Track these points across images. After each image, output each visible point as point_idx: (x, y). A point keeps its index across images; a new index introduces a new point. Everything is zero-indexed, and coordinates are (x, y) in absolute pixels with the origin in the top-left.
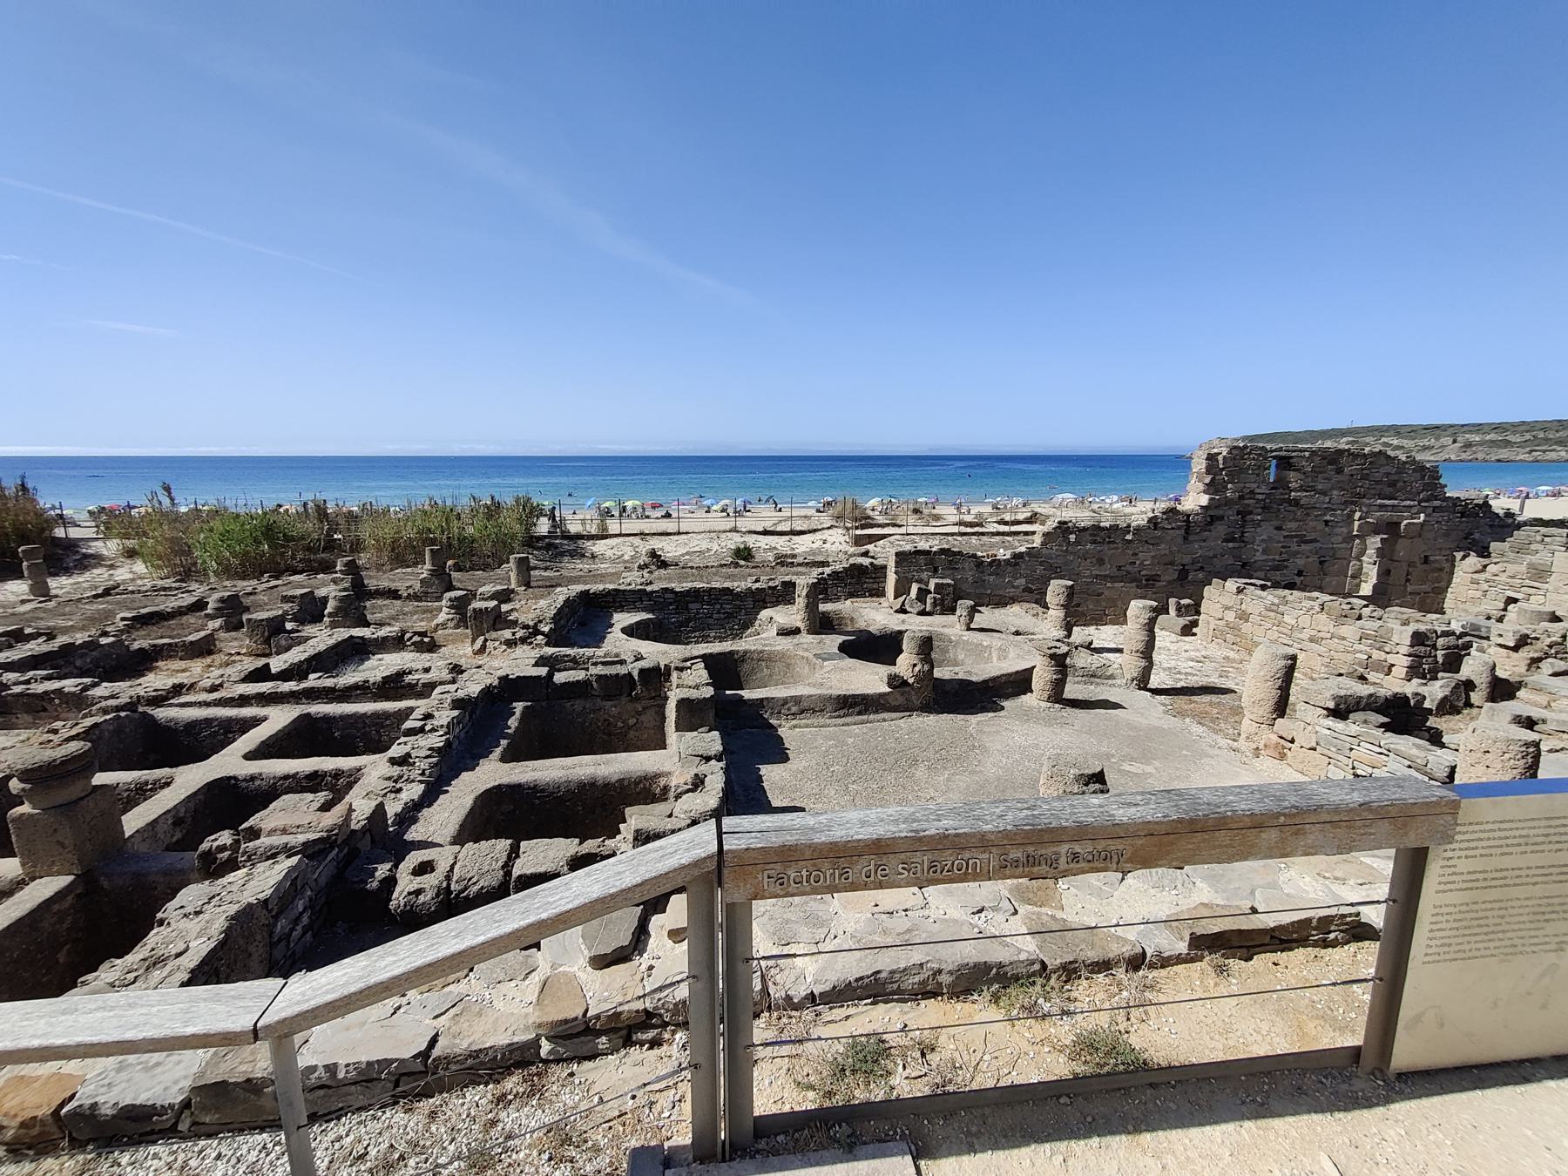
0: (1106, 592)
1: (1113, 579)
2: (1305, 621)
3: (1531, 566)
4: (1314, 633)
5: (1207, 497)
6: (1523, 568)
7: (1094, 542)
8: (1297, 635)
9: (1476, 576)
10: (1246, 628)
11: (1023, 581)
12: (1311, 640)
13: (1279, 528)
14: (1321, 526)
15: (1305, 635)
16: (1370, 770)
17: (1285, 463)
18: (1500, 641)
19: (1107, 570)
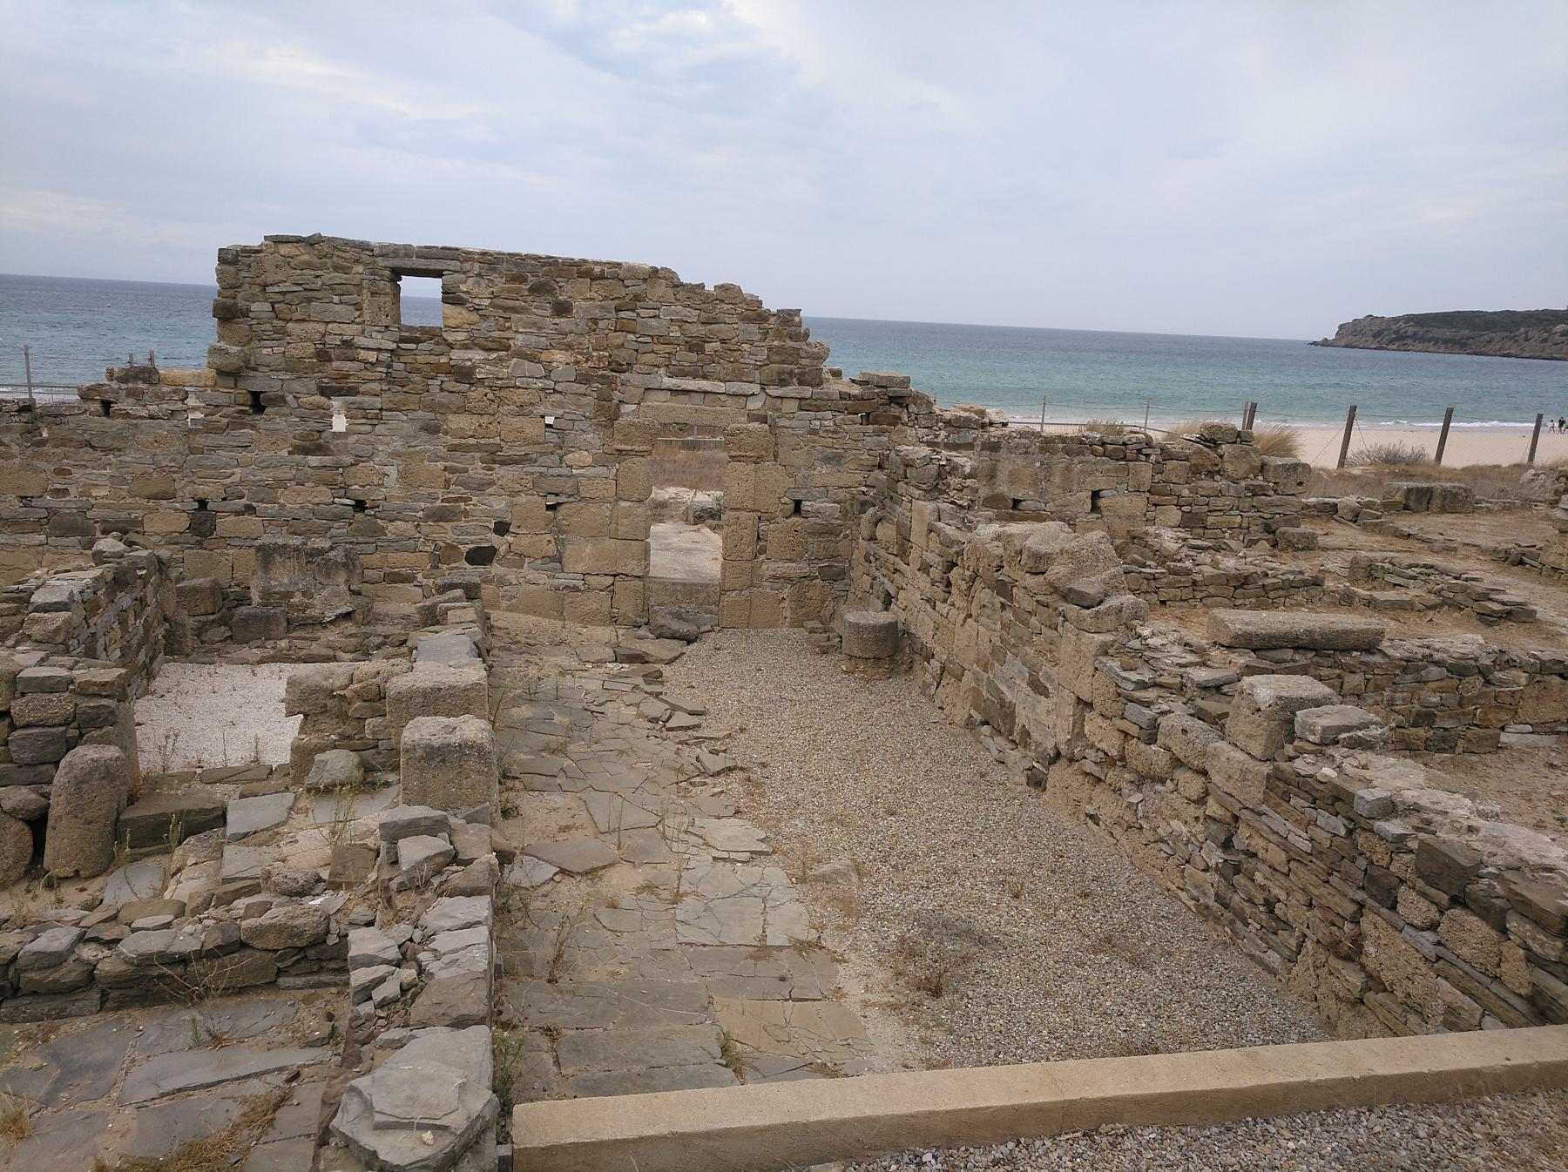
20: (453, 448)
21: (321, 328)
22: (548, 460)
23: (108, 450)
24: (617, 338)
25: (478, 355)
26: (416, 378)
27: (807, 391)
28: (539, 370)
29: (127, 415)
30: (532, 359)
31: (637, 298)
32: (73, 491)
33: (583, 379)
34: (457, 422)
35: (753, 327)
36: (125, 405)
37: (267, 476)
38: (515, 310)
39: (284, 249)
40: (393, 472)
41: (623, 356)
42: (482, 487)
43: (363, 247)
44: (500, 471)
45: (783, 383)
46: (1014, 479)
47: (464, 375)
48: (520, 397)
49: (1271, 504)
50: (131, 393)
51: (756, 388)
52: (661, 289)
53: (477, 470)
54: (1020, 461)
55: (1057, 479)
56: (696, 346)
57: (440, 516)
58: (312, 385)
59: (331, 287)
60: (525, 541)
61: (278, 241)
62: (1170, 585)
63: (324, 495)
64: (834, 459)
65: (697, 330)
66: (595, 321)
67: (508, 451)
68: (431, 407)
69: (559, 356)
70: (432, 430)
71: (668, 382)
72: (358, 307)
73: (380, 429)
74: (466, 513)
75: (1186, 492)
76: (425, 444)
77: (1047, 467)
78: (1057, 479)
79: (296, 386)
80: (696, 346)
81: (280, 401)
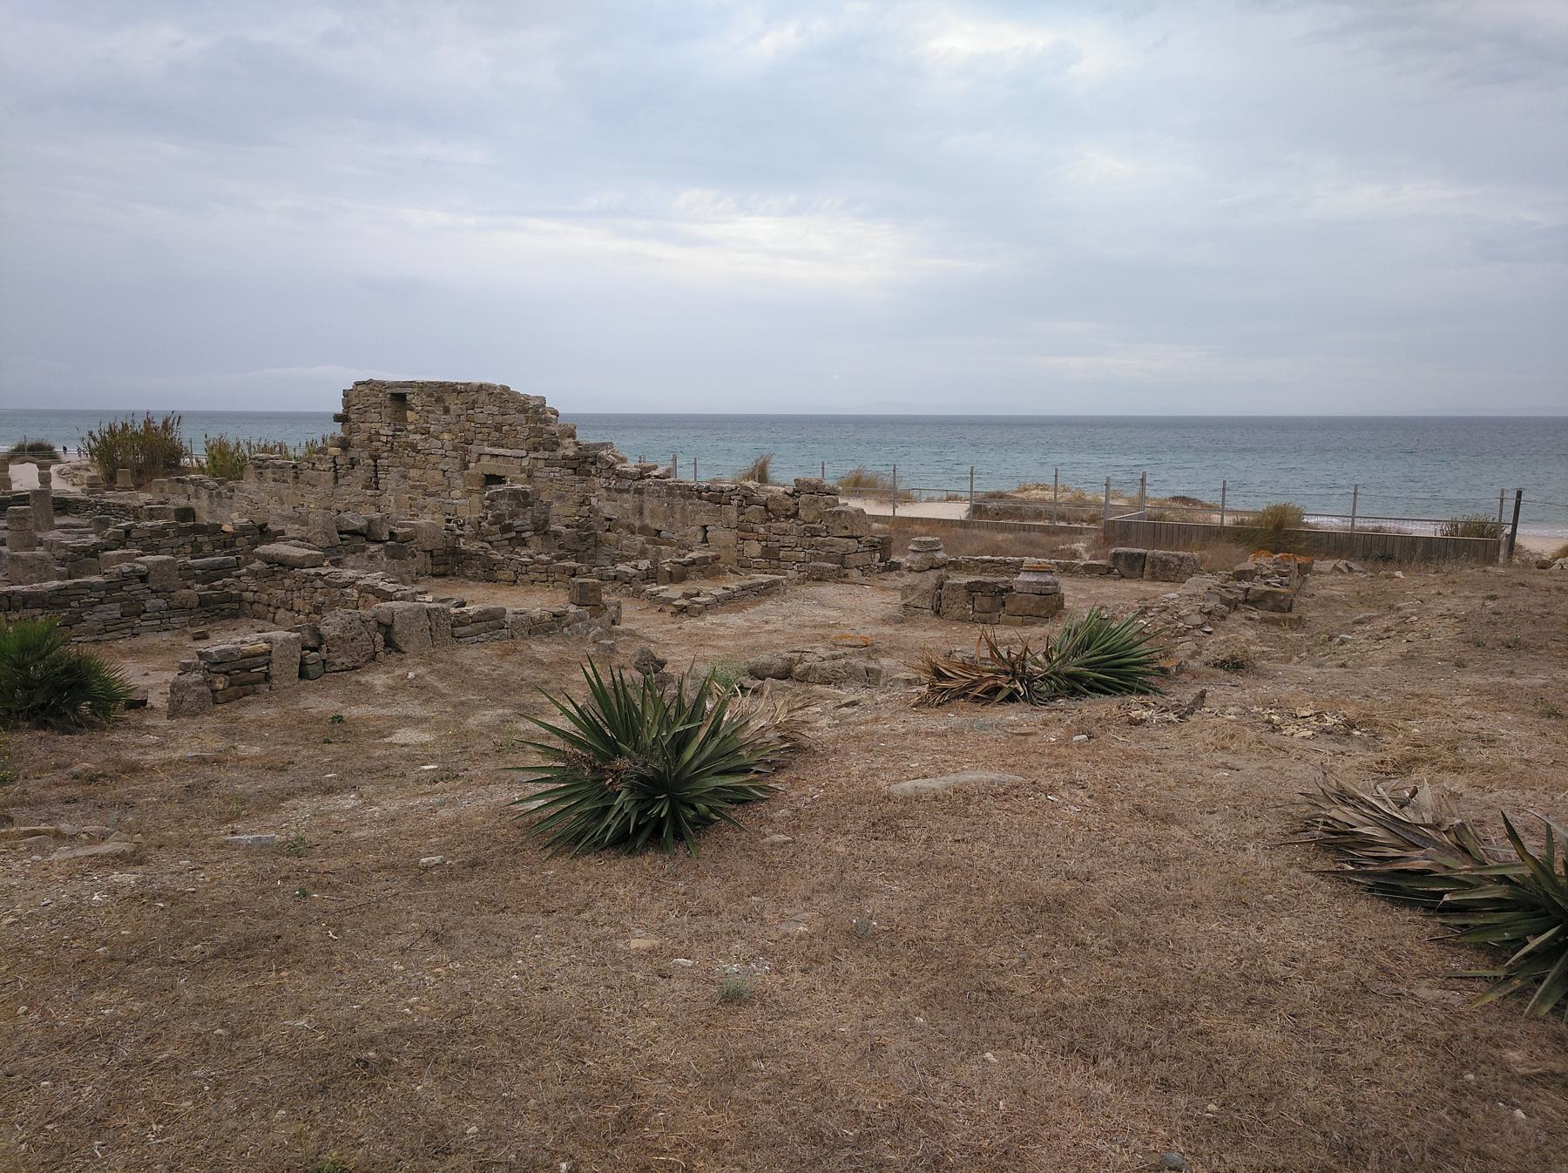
13: (405, 477)
14: (439, 477)
20: (412, 487)
25: (418, 437)
30: (437, 438)
31: (474, 402)
33: (455, 449)
34: (413, 473)
35: (522, 416)
41: (470, 435)
44: (429, 500)
45: (536, 450)
46: (653, 515)
48: (432, 459)
49: (824, 544)
50: (320, 459)
51: (524, 453)
52: (483, 396)
53: (420, 501)
54: (655, 501)
55: (678, 516)
56: (498, 428)
61: (357, 384)
62: (534, 570)
65: (499, 419)
67: (432, 489)
68: (405, 465)
69: (446, 436)
75: (762, 530)
76: (405, 486)
77: (671, 506)
78: (678, 516)
80: (498, 428)
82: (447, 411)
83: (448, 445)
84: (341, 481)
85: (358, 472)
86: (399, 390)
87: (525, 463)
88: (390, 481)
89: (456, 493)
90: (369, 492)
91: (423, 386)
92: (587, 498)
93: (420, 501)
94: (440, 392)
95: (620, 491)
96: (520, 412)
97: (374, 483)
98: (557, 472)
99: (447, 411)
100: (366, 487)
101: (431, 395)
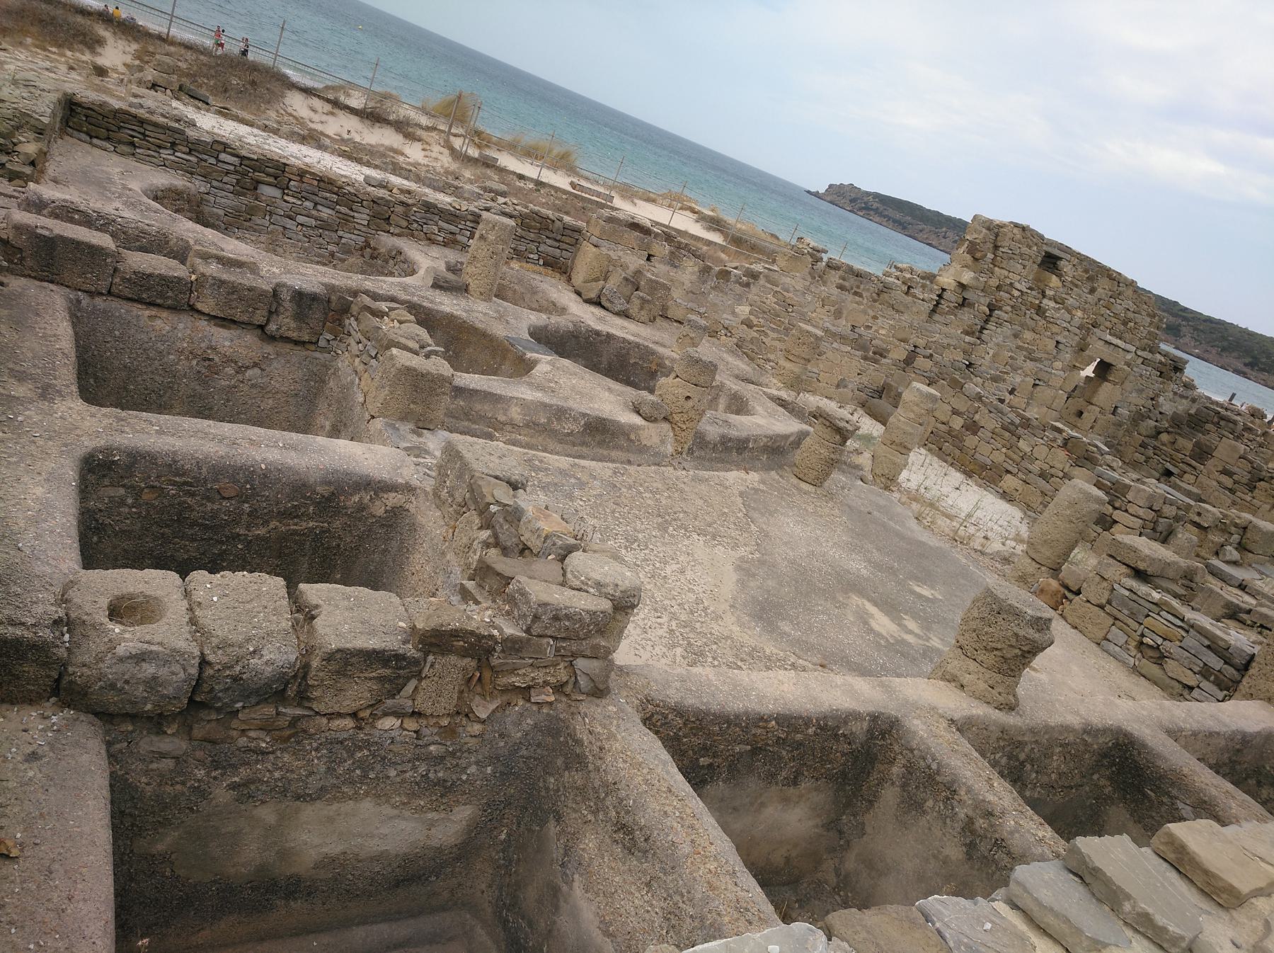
0: (829, 354)
1: (842, 338)
2: (1041, 452)
3: (1197, 445)
4: (1046, 467)
5: (972, 274)
6: (1189, 445)
7: (841, 287)
8: (1026, 464)
9: (1147, 440)
10: (971, 441)
11: (747, 309)
12: (1042, 475)
14: (1051, 345)
15: (1035, 467)
16: (1160, 641)
17: (1051, 259)
18: (1197, 519)
19: (843, 326)
20: (1018, 347)
21: (1006, 273)
22: (1046, 363)
23: (897, 311)
24: (1103, 310)
25: (1052, 304)
26: (1023, 308)
27: (1149, 356)
28: (1067, 316)
29: (915, 296)
30: (1069, 312)
32: (874, 328)
34: (1028, 335)
35: (1149, 320)
36: (916, 291)
37: (945, 341)
38: (1077, 286)
39: (1016, 231)
40: (991, 352)
42: (1015, 369)
43: (1042, 237)
45: (1144, 350)
47: (1040, 311)
48: (1055, 329)
50: (924, 286)
56: (1125, 324)
57: (995, 379)
58: (988, 300)
59: (1021, 255)
60: (1017, 400)
61: (1016, 225)
63: (959, 356)
64: (1140, 391)
65: (1130, 315)
66: (1099, 300)
68: (1022, 325)
69: (1079, 313)
70: (1016, 336)
71: (1109, 338)
72: (1024, 267)
73: (999, 330)
74: (1004, 380)
76: (1012, 344)
79: (982, 300)
81: (971, 305)
82: (1092, 291)
83: (1077, 321)
84: (937, 317)
85: (966, 316)
86: (1056, 252)
87: (1129, 357)
88: (997, 336)
89: (1058, 364)
90: (968, 339)
91: (1082, 258)
92: (1158, 396)
93: (1020, 362)
94: (1094, 272)
95: (1182, 397)
96: (1149, 315)
97: (978, 332)
98: (1147, 371)
99: (1092, 291)
100: (967, 333)
101: (1086, 271)
